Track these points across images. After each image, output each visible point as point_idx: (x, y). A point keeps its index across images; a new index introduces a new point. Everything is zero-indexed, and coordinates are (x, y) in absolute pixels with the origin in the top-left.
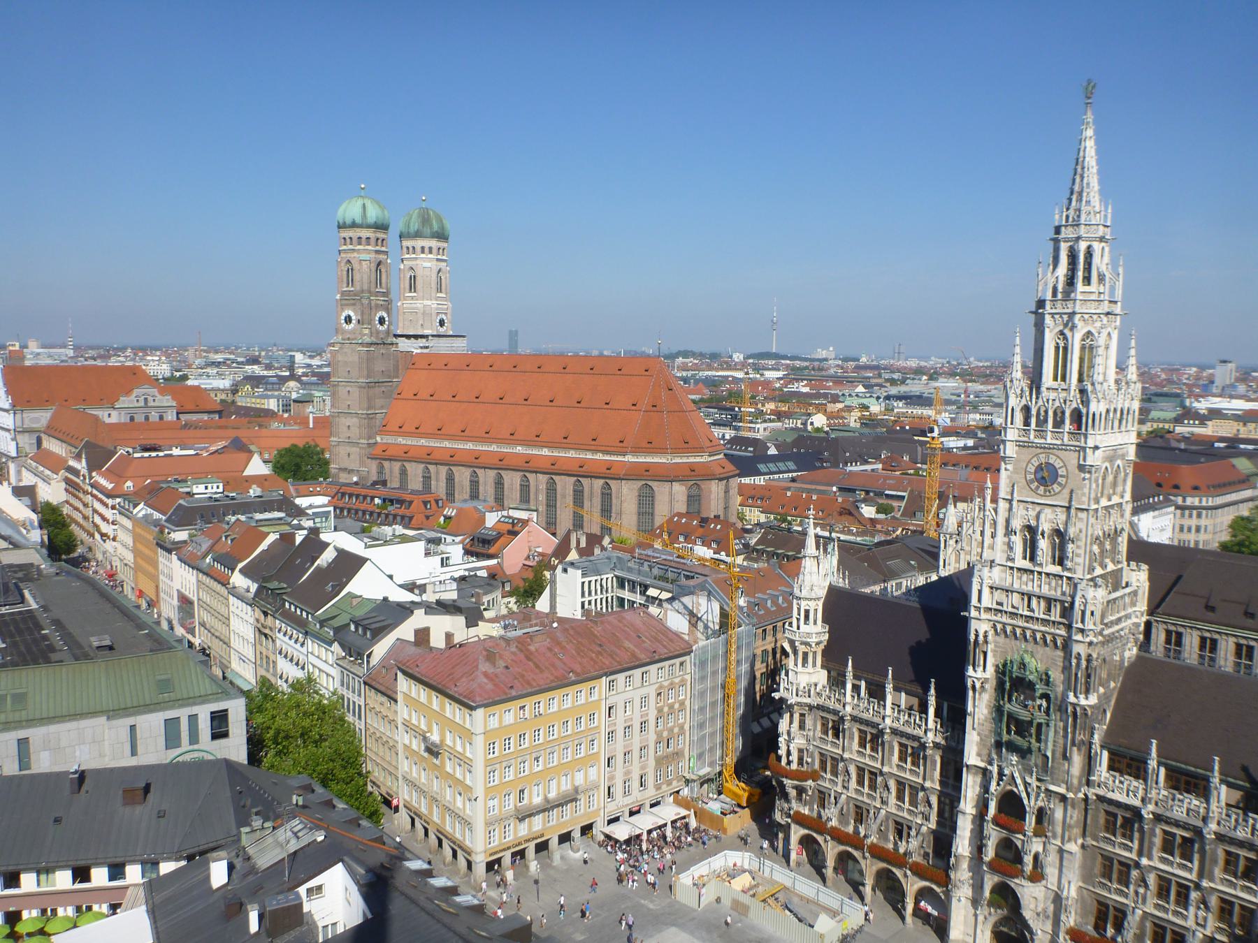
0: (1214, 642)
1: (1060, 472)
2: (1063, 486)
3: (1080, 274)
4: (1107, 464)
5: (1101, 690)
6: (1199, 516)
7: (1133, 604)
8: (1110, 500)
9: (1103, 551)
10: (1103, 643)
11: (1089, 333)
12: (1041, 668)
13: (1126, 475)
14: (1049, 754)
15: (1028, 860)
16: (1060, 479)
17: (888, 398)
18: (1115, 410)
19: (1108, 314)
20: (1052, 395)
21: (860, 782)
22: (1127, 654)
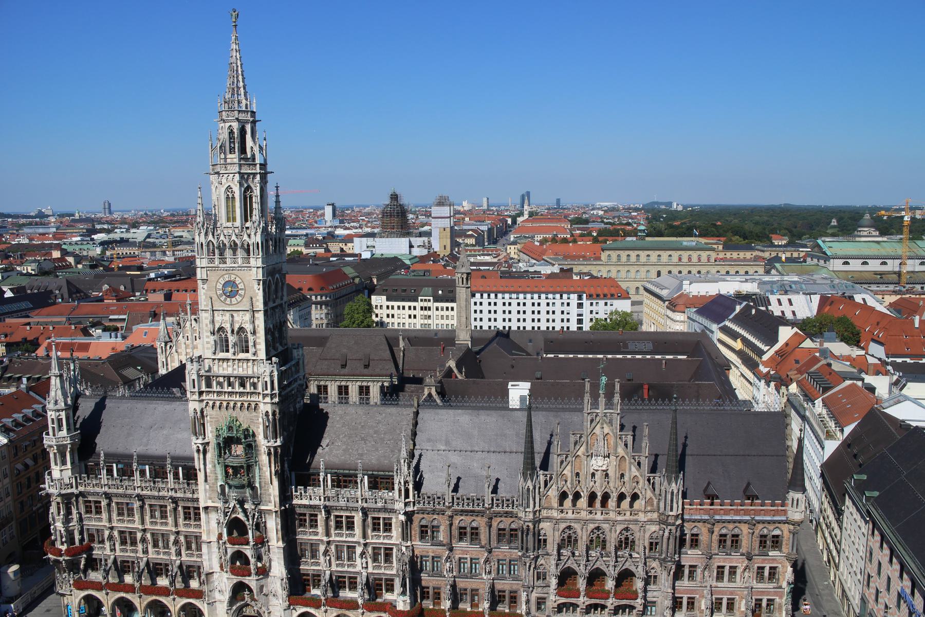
4: (270, 278)
5: (285, 434)
12: (244, 426)
14: (257, 485)
15: (252, 561)
17: (102, 243)
21: (123, 542)
22: (298, 406)
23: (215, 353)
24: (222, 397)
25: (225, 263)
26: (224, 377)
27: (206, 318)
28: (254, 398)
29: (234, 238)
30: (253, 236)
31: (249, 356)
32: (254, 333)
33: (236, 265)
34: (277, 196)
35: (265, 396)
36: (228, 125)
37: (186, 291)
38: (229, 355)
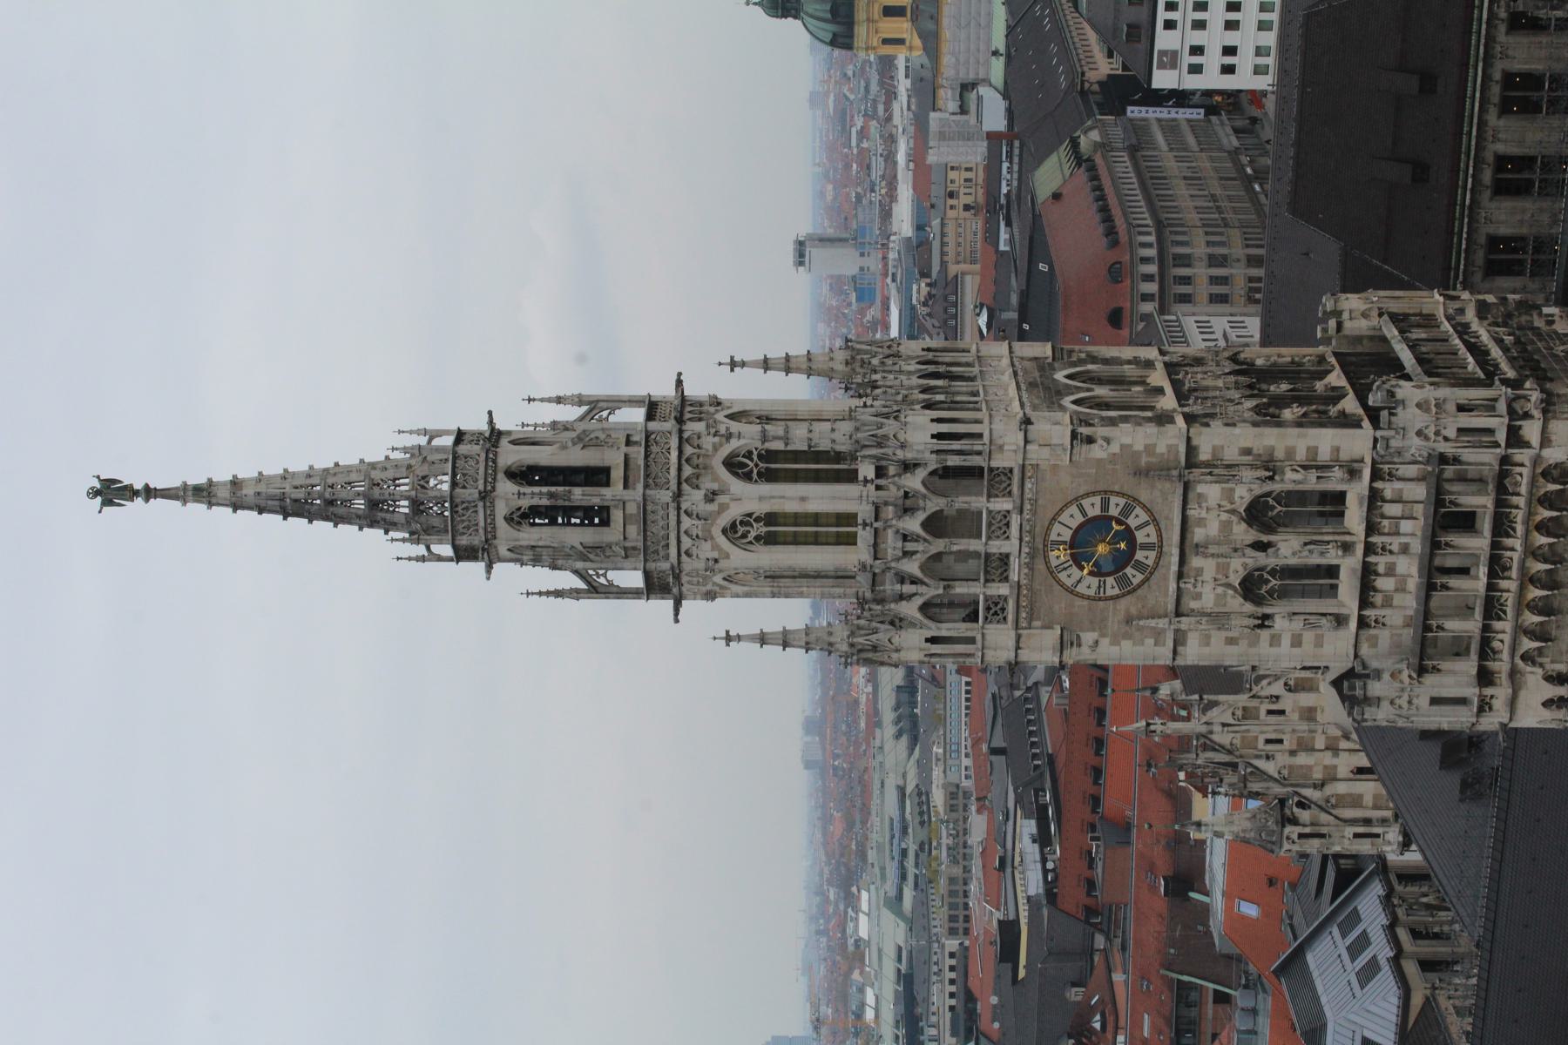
0: (1501, 161)
1: (1094, 512)
2: (1133, 502)
3: (579, 495)
4: (1067, 401)
6: (1184, 260)
7: (1428, 321)
8: (1160, 391)
9: (1301, 401)
10: (1542, 378)
11: (732, 464)
13: (1093, 359)
16: (1114, 511)
18: (925, 390)
19: (680, 420)
20: (891, 544)
23: (1340, 620)
24: (1509, 600)
25: (1004, 559)
26: (1430, 588)
27: (1206, 641)
28: (1523, 477)
29: (913, 524)
30: (909, 455)
31: (1356, 493)
32: (1270, 466)
33: (1015, 520)
34: (766, 365)
35: (1515, 438)
36: (501, 523)
37: (1099, 743)
38: (1349, 566)
